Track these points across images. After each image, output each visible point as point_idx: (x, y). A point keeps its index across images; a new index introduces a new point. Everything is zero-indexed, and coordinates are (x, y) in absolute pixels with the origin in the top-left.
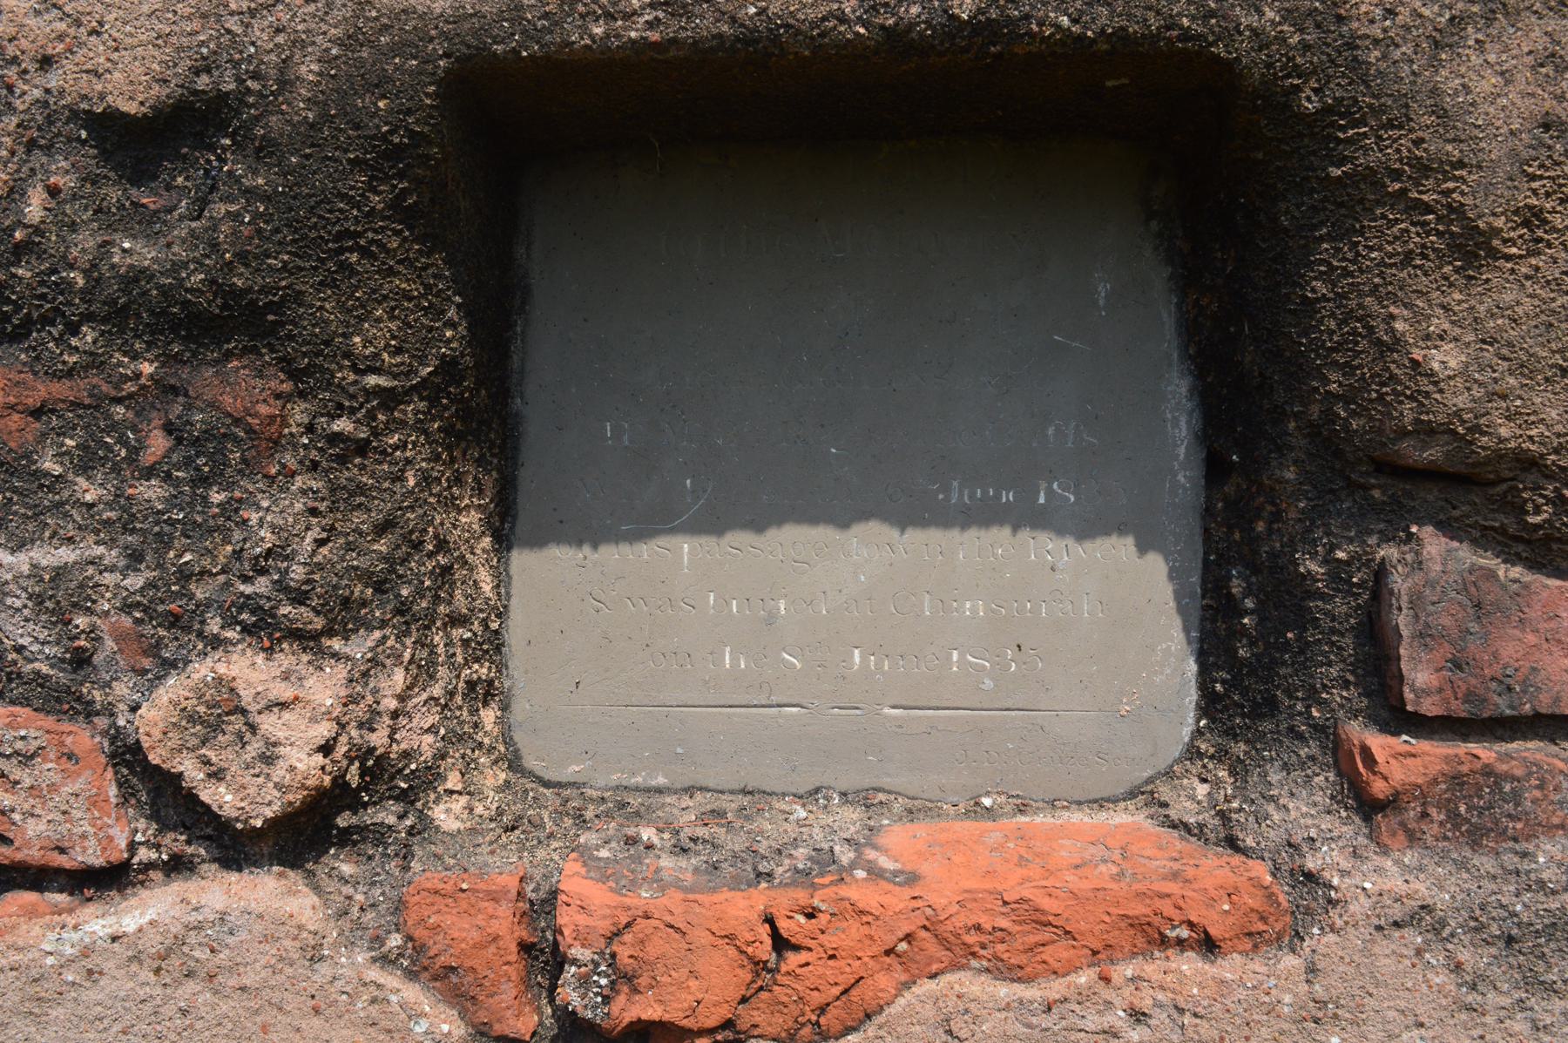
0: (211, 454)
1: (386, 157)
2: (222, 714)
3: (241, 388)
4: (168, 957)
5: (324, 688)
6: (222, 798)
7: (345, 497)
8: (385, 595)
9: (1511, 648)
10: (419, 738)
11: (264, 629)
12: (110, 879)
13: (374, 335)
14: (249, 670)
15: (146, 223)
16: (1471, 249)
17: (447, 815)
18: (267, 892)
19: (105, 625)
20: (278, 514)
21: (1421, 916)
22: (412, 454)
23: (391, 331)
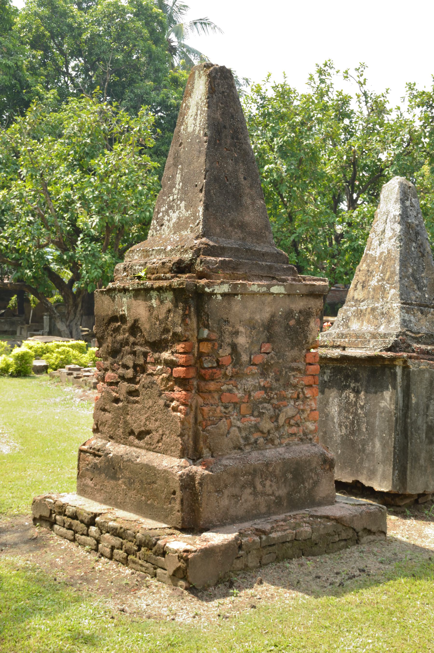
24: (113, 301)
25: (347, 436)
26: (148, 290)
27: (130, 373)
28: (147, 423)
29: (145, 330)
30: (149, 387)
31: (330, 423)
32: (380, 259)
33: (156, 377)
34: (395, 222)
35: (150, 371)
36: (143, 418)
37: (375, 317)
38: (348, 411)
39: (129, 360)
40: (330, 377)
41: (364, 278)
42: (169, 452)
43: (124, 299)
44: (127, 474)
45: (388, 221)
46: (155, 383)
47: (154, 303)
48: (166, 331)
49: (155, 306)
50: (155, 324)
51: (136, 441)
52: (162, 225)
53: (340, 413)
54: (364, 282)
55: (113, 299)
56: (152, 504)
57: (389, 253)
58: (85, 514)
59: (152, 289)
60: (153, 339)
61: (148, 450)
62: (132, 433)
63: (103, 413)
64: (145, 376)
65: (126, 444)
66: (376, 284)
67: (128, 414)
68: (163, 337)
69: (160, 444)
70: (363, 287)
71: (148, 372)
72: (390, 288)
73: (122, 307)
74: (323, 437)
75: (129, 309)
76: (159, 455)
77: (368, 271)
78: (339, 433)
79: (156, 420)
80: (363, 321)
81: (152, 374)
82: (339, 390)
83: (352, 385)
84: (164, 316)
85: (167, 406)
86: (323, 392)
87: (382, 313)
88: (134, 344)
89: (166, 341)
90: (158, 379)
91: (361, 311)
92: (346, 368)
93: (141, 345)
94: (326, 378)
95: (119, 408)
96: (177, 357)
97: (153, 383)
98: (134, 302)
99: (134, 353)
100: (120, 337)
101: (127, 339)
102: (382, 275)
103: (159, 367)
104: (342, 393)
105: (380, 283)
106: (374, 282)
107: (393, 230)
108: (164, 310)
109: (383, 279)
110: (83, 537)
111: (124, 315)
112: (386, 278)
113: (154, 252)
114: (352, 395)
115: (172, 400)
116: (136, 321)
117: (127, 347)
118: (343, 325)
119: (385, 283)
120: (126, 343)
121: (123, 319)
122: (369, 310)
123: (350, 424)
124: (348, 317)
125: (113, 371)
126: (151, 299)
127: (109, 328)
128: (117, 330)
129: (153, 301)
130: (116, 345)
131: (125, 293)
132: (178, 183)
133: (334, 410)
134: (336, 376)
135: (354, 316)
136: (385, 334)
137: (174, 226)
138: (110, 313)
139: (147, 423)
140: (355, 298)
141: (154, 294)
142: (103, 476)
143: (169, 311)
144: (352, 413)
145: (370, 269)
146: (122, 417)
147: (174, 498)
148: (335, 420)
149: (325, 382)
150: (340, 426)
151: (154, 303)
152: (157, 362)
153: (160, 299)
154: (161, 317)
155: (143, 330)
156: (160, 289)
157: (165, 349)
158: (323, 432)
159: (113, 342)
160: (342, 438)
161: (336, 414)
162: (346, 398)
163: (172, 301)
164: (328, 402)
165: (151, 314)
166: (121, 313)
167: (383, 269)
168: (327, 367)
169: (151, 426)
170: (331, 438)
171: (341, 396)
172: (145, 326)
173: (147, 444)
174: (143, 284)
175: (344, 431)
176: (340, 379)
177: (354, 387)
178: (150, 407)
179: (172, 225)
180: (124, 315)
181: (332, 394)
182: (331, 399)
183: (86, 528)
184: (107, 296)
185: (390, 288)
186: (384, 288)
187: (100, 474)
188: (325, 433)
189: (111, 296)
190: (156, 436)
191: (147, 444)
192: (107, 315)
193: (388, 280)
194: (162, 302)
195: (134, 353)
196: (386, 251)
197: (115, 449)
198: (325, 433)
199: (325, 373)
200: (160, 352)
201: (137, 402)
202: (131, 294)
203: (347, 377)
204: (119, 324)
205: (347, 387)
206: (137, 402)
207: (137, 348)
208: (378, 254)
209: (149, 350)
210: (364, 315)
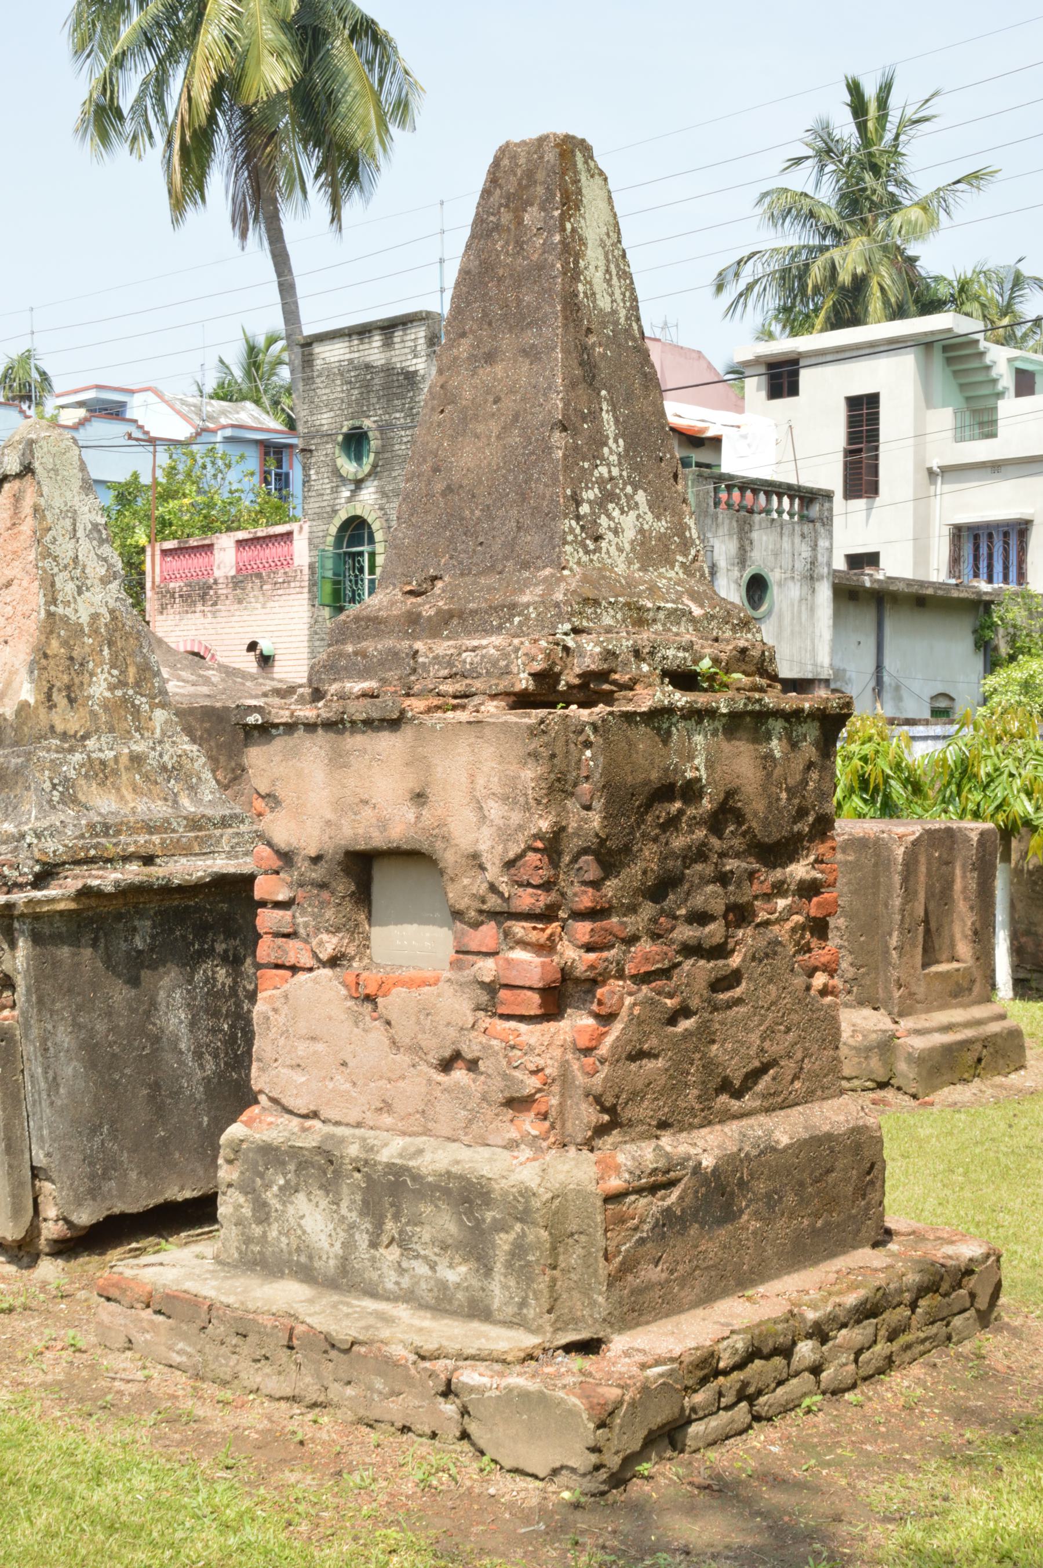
0: (323, 905)
1: (339, 864)
2: (321, 943)
3: (325, 895)
4: (315, 981)
5: (335, 940)
6: (321, 956)
7: (339, 912)
8: (353, 929)
9: (466, 940)
10: (351, 950)
11: (328, 931)
12: (311, 970)
13: (341, 888)
14: (325, 937)
15: (315, 871)
16: (452, 880)
17: (355, 964)
18: (327, 972)
19: (311, 929)
20: (329, 913)
21: (449, 980)
22: (348, 905)
23: (344, 886)
24: (666, 741)
25: (220, 1075)
26: (763, 716)
27: (714, 931)
28: (767, 1044)
29: (755, 814)
30: (767, 955)
31: (169, 1057)
32: (96, 631)
33: (777, 927)
34: (102, 542)
35: (762, 916)
36: (754, 1038)
37: (146, 778)
38: (215, 1014)
39: (710, 897)
40: (153, 937)
41: (66, 678)
42: (819, 1093)
43: (699, 739)
44: (761, 1187)
45: (80, 533)
46: (780, 943)
47: (776, 747)
48: (802, 813)
49: (778, 754)
50: (779, 799)
51: (735, 1105)
52: (598, 538)
53: (193, 1024)
54: (69, 688)
55: (666, 737)
56: (827, 1224)
57: (114, 619)
58: (780, 1327)
59: (778, 714)
60: (776, 836)
61: (768, 1110)
62: (725, 1086)
63: (633, 1067)
64: (749, 931)
65: (710, 1123)
66: (108, 694)
67: (713, 1042)
68: (796, 829)
69: (797, 1085)
70: (71, 701)
71: (759, 920)
72: (152, 707)
73: (691, 758)
74: (151, 1098)
75: (710, 765)
76: (800, 1108)
77: (71, 659)
78: (199, 1074)
79: (788, 1030)
80: (118, 790)
81: (766, 923)
82: (184, 965)
83: (220, 947)
84: (798, 777)
85: (808, 988)
86: (134, 982)
87: (164, 768)
88: (722, 855)
89: (799, 837)
90: (781, 932)
91: (103, 763)
92: (198, 909)
93: (737, 855)
94: (139, 943)
95: (687, 1034)
96: (822, 872)
97: (776, 943)
98: (727, 747)
99: (723, 879)
100: (678, 842)
101: (704, 844)
102: (115, 672)
103: (782, 903)
104: (193, 971)
105: (119, 693)
106: (99, 688)
107: (105, 560)
108: (798, 764)
109: (122, 684)
110: (780, 1391)
111: (699, 780)
112: (131, 680)
113: (661, 615)
114: (221, 972)
115: (811, 973)
116: (730, 794)
117: (699, 867)
118: (62, 801)
119: (131, 692)
120: (700, 854)
121: (691, 791)
122: (124, 760)
123: (224, 1042)
124: (67, 779)
125: (655, 936)
126: (769, 739)
127: (649, 818)
128: (672, 823)
129: (774, 743)
130: (670, 864)
131: (700, 722)
132: (611, 436)
133: (175, 1018)
134: (171, 931)
135: (86, 776)
136: (224, 817)
137: (633, 550)
138: (654, 775)
139: (767, 1044)
140: (60, 728)
141: (777, 726)
142: (694, 1230)
143: (810, 766)
144: (227, 1016)
145: (75, 654)
146: (697, 1056)
147: (872, 1183)
148: (183, 1046)
149: (140, 952)
150: (198, 1055)
151: (776, 747)
152: (779, 889)
153: (790, 739)
154: (791, 782)
155: (749, 816)
156: (795, 716)
157: (793, 858)
158: (150, 1086)
159: (663, 859)
160: (207, 1087)
161: (184, 1029)
162: (206, 982)
163: (816, 744)
164: (153, 1004)
165: (769, 775)
166: (689, 775)
167: (114, 656)
168: (141, 914)
169: (773, 1049)
170: (176, 1094)
171: (190, 981)
172: (755, 806)
173: (764, 1097)
174: (759, 701)
175: (210, 1066)
176: (184, 937)
177: (226, 951)
178: (773, 1004)
179: (627, 547)
180: (699, 780)
181: (166, 982)
182: (162, 994)
183: (784, 1362)
184: (642, 728)
185: (152, 707)
186: (133, 706)
187: (683, 1231)
188: (156, 1086)
189: (658, 729)
190: (789, 1066)
191: (764, 1097)
192: (647, 782)
193: (137, 684)
194: (794, 745)
195: (723, 879)
196: (103, 611)
197: (706, 1146)
198: (156, 1086)
199: (135, 929)
200: (784, 866)
201: (738, 1001)
202: (718, 724)
203: (202, 930)
204: (678, 805)
205: (202, 955)
206: (738, 1001)
207: (731, 864)
208: (85, 619)
209: (756, 866)
210: (115, 772)
